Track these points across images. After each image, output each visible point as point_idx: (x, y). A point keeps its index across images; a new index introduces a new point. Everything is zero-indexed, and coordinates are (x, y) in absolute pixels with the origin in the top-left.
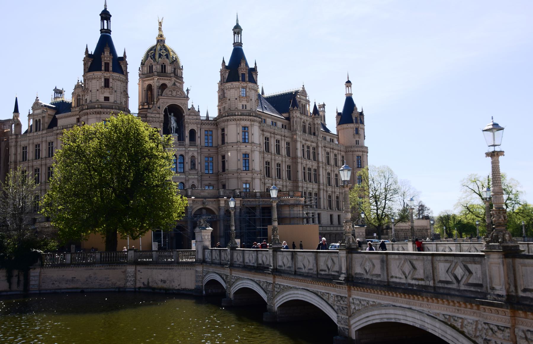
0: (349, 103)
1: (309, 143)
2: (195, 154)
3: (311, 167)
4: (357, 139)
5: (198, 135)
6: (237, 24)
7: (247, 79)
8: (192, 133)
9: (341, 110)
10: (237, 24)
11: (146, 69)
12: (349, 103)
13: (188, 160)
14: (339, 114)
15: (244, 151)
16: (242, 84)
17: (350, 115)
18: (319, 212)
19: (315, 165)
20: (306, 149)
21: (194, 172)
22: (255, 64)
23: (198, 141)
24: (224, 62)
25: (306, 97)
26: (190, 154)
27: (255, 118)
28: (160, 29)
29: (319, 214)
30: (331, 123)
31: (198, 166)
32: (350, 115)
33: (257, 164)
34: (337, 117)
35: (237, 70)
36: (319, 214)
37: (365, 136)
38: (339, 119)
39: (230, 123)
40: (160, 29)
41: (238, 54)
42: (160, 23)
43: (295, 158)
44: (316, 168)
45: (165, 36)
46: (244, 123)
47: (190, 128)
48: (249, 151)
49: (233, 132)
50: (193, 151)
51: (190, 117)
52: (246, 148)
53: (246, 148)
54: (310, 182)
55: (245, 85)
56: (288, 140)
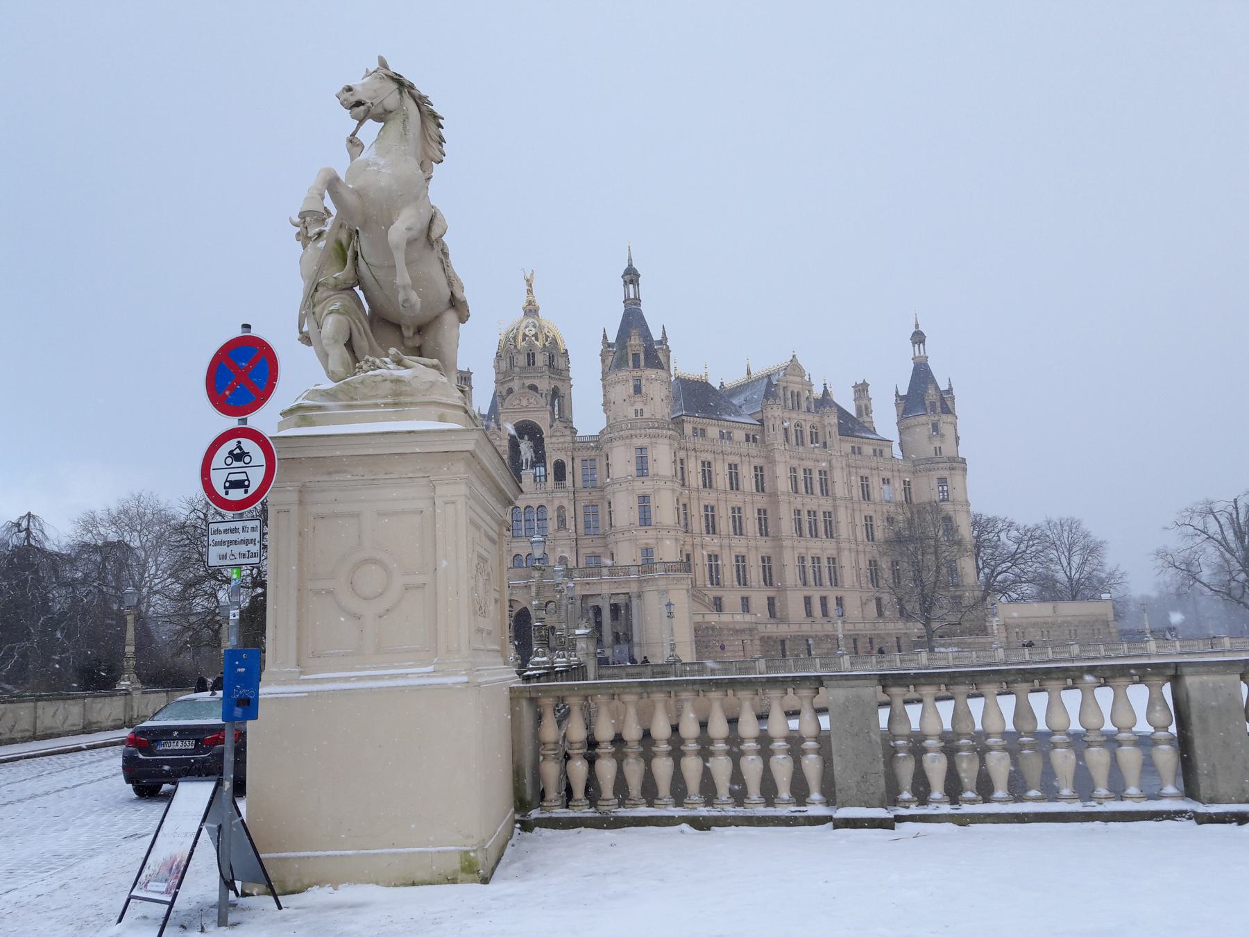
0: (922, 374)
1: (808, 464)
2: (565, 503)
3: (800, 507)
4: (938, 444)
5: (568, 469)
6: (630, 265)
7: (642, 363)
8: (560, 469)
9: (904, 391)
10: (630, 265)
11: (504, 365)
12: (922, 374)
13: (551, 513)
14: (902, 398)
15: (640, 492)
16: (635, 374)
17: (924, 398)
18: (840, 594)
19: (826, 504)
20: (801, 475)
21: (563, 533)
22: (664, 333)
23: (569, 477)
24: (605, 336)
25: (803, 377)
26: (557, 503)
27: (659, 431)
28: (530, 291)
29: (840, 601)
30: (885, 421)
31: (570, 524)
32: (924, 398)
33: (665, 511)
34: (897, 405)
35: (635, 348)
36: (840, 601)
37: (957, 438)
38: (901, 409)
39: (615, 443)
40: (530, 291)
41: (633, 319)
42: (529, 282)
43: (774, 496)
44: (830, 509)
45: (538, 302)
46: (639, 442)
47: (555, 458)
48: (648, 492)
49: (621, 461)
50: (562, 498)
51: (554, 440)
52: (644, 487)
53: (644, 487)
54: (801, 536)
55: (639, 374)
56: (758, 462)
